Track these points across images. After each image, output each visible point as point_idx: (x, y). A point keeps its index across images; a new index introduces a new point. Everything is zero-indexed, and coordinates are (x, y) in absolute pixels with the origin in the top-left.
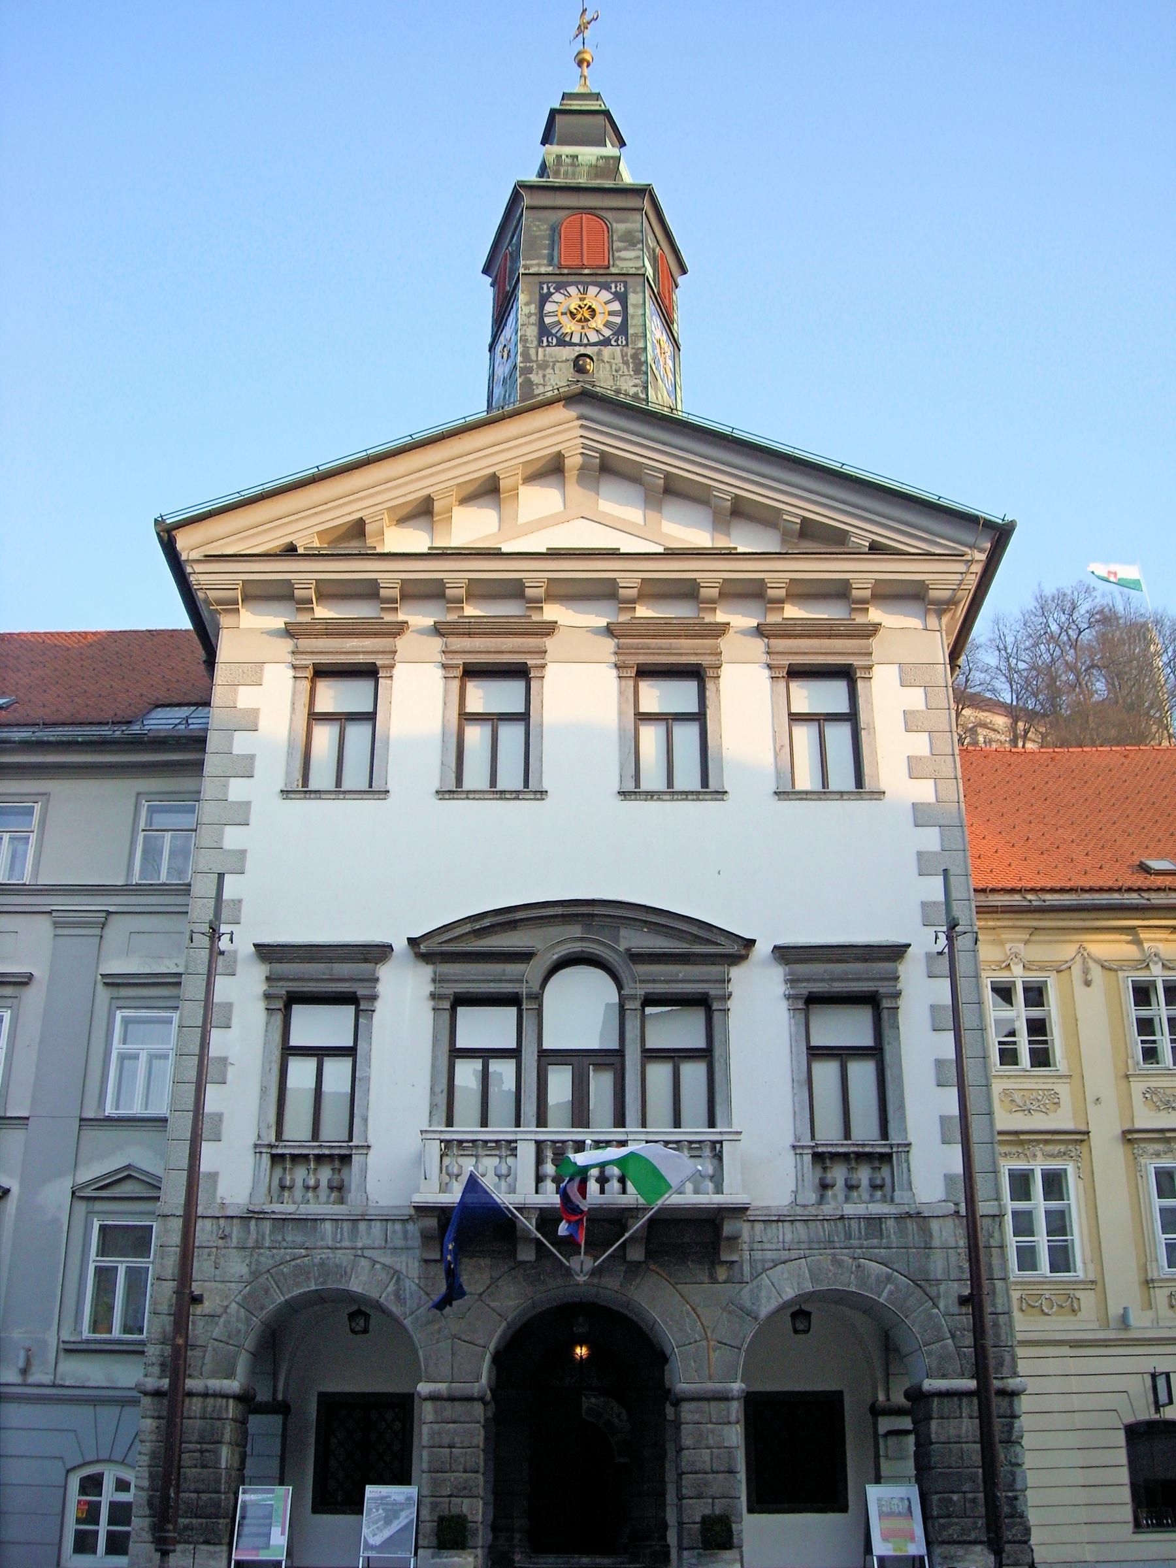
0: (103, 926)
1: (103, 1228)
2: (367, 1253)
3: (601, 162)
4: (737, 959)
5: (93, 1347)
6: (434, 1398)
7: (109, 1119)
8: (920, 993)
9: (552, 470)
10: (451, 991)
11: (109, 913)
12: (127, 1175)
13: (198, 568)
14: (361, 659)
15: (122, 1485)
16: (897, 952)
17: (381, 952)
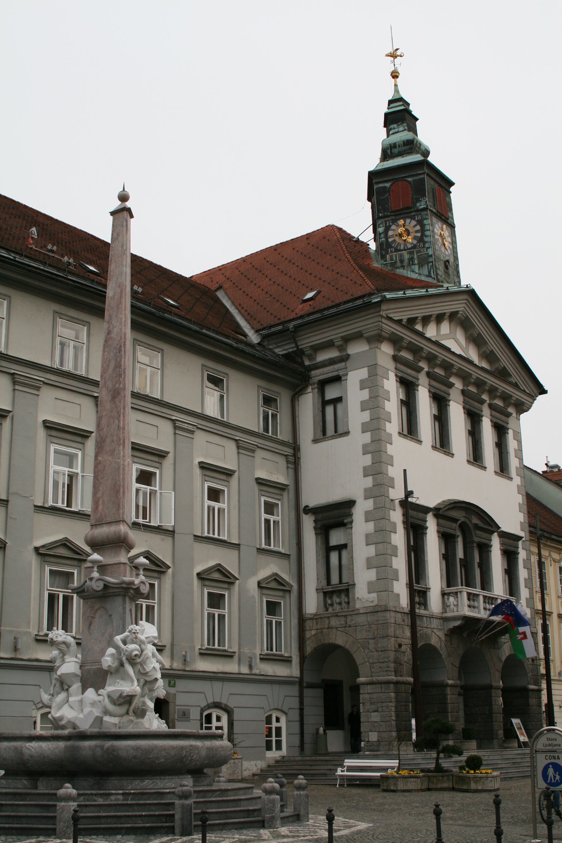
0: (253, 451)
1: (267, 601)
2: (435, 630)
3: (425, 152)
4: (493, 532)
5: (268, 657)
6: (451, 686)
7: (263, 550)
8: (522, 555)
9: (453, 316)
10: (442, 530)
11: (258, 447)
12: (276, 578)
13: (384, 321)
14: (410, 379)
15: (278, 720)
16: (519, 538)
17: (426, 510)
